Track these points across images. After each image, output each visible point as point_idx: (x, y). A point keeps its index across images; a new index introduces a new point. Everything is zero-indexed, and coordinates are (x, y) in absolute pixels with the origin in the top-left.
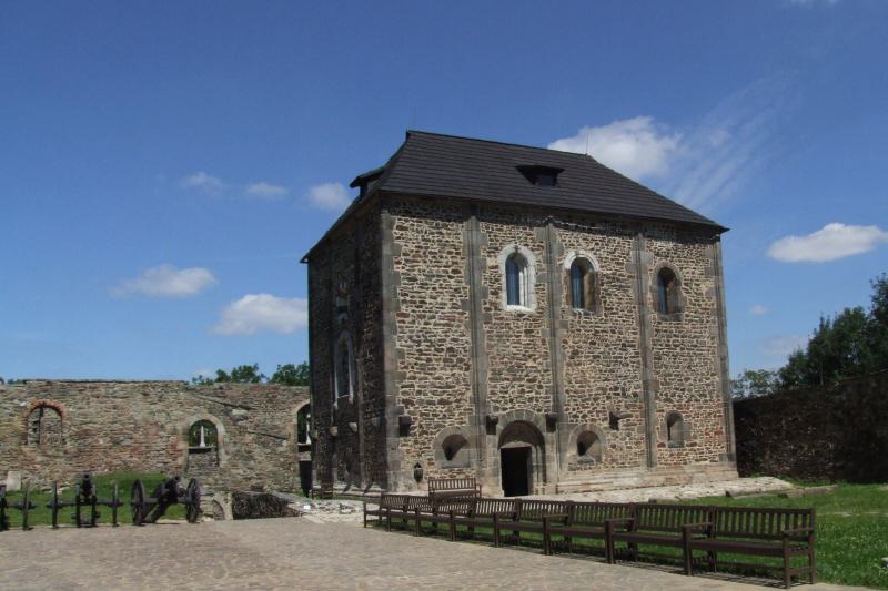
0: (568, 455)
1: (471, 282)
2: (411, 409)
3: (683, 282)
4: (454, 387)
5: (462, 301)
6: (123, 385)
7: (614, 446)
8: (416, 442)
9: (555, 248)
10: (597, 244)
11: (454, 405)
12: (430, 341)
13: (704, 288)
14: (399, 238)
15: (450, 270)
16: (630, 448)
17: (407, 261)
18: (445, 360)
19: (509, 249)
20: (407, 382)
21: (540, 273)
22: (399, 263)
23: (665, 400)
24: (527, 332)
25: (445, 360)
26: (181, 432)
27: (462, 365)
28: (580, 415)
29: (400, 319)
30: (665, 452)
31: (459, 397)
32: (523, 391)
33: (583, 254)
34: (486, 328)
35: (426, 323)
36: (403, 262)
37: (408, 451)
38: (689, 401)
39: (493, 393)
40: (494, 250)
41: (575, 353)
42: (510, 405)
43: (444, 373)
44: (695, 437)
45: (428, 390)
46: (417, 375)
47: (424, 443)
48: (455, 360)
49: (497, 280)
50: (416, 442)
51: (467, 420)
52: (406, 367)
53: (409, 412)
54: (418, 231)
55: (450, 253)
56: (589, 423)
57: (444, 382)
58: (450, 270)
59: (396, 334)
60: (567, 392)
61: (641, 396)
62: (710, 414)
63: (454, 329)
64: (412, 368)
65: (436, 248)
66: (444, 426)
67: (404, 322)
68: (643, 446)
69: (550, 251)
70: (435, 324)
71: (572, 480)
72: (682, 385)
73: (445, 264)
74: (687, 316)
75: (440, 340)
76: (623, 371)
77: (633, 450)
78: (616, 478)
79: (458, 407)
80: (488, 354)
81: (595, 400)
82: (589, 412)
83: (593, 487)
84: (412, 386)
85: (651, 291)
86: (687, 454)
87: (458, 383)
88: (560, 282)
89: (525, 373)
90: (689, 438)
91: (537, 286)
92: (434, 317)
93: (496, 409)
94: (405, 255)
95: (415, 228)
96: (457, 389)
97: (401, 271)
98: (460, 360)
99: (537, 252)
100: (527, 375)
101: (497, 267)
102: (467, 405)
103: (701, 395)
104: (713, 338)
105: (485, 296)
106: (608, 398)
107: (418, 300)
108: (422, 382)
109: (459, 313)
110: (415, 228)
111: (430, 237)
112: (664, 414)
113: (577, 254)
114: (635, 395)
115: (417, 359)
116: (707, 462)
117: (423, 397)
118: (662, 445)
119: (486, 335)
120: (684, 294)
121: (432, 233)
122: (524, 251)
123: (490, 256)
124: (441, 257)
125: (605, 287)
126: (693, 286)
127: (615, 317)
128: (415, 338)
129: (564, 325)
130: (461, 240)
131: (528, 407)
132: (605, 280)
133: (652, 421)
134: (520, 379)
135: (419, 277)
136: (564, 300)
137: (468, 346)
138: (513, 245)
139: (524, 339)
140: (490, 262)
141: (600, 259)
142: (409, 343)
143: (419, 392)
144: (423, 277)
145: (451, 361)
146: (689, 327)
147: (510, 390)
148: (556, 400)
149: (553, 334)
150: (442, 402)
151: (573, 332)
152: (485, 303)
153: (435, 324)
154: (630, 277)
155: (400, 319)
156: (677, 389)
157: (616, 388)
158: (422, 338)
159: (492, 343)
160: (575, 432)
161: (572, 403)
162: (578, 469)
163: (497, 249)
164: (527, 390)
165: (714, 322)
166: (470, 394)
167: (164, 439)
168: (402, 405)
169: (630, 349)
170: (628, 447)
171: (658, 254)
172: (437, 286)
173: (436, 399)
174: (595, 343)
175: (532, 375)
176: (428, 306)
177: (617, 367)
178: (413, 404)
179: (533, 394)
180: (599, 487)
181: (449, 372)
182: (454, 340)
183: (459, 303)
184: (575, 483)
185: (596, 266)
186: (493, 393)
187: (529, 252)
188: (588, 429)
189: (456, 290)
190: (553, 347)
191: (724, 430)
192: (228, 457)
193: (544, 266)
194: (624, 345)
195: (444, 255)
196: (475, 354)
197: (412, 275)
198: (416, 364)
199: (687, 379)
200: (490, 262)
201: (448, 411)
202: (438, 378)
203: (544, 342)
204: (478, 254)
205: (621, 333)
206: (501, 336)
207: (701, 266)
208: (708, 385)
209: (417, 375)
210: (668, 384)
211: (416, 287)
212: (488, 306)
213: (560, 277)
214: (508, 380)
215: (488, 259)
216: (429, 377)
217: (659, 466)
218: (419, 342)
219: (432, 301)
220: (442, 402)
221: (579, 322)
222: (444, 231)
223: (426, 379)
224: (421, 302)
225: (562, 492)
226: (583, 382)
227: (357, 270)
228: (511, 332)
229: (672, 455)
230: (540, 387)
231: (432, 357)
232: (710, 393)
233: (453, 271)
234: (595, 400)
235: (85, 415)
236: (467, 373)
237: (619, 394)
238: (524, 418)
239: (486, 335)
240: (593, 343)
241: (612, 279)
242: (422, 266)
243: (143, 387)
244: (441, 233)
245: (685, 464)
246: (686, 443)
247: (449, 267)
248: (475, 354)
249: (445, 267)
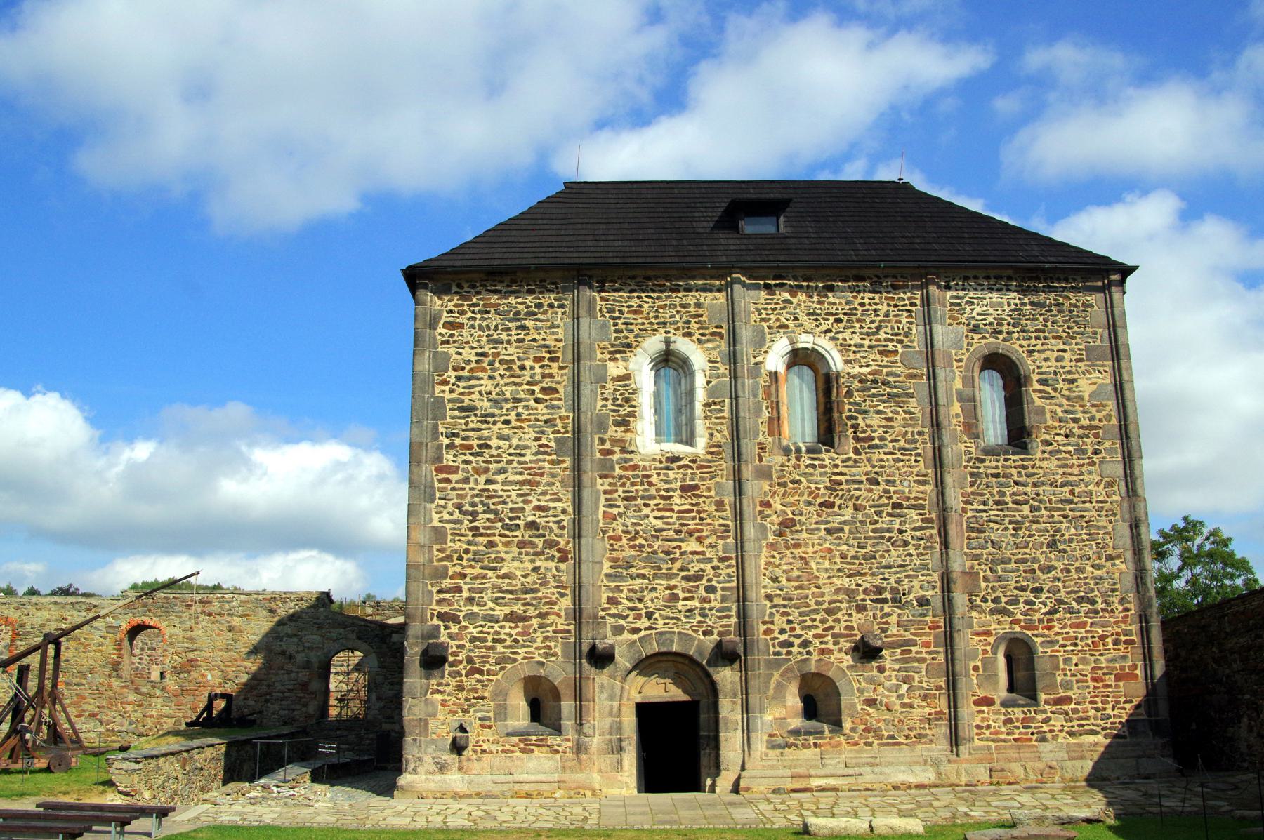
0: (768, 718)
1: (576, 407)
2: (454, 629)
3: (1035, 377)
4: (537, 591)
5: (557, 441)
6: (243, 597)
7: (871, 703)
8: (460, 688)
9: (745, 334)
10: (839, 321)
11: (535, 622)
12: (496, 512)
13: (1085, 387)
14: (443, 343)
15: (537, 389)
16: (911, 706)
17: (459, 378)
18: (521, 545)
19: (654, 344)
20: (447, 583)
21: (714, 382)
22: (445, 383)
23: (992, 612)
24: (684, 489)
25: (521, 545)
26: (316, 665)
27: (553, 552)
28: (797, 641)
29: (441, 476)
30: (995, 717)
31: (544, 609)
32: (675, 597)
33: (806, 341)
34: (602, 485)
35: (488, 482)
36: (453, 380)
37: (444, 703)
38: (1053, 611)
39: (612, 601)
40: (624, 349)
41: (788, 524)
42: (644, 623)
43: (517, 566)
44: (1067, 685)
45: (487, 596)
46: (468, 571)
47: (476, 690)
48: (540, 543)
49: (627, 400)
50: (460, 688)
51: (559, 650)
52: (449, 558)
53: (450, 636)
54: (481, 328)
55: (538, 359)
56: (815, 657)
57: (517, 584)
58: (537, 389)
59: (432, 502)
60: (769, 597)
61: (937, 602)
62: (1103, 638)
63: (540, 489)
64: (460, 558)
65: (512, 352)
66: (515, 660)
67: (448, 481)
68: (942, 704)
69: (733, 340)
70: (505, 483)
71: (772, 767)
72: (1035, 580)
73: (528, 378)
74: (1048, 443)
75: (512, 510)
76: (895, 556)
77: (916, 712)
78: (872, 765)
79: (541, 626)
80: (604, 532)
82: (816, 636)
83: (815, 782)
84: (459, 590)
85: (961, 398)
86: (1046, 721)
87: (544, 583)
88: (755, 396)
89: (678, 565)
90: (1052, 686)
91: (707, 405)
92: (503, 471)
93: (618, 630)
94: (455, 369)
95: (476, 323)
96: (540, 594)
97: (447, 396)
98: (551, 544)
99: (710, 345)
100: (682, 569)
101: (627, 377)
102: (561, 624)
103: (1080, 600)
104: (1110, 485)
106: (861, 608)
107: (475, 442)
108: (477, 584)
109: (552, 462)
110: (476, 323)
111: (504, 336)
112: (991, 640)
113: (792, 343)
114: (923, 602)
115: (469, 543)
117: (476, 609)
119: (603, 497)
120: (1038, 402)
121: (509, 329)
122: (684, 346)
123: (615, 360)
124: (522, 368)
125: (857, 397)
127: (876, 455)
128: (468, 508)
129: (764, 474)
130: (561, 336)
131: (684, 626)
132: (856, 385)
133: (958, 654)
134: (669, 576)
135: (478, 404)
136: (763, 428)
137: (567, 520)
138: (660, 336)
139: (678, 502)
140: (614, 369)
141: (845, 348)
142: (457, 515)
143: (470, 600)
144: (487, 404)
145: (533, 545)
146: (1052, 464)
147: (648, 596)
148: (743, 614)
149: (739, 490)
150: (513, 618)
151: (784, 485)
152: (602, 441)
154: (911, 376)
155: (441, 476)
156: (1023, 589)
157: (879, 590)
158: (480, 508)
159: (615, 511)
160: (782, 675)
161: (780, 621)
162: (789, 746)
163: (629, 346)
164: (682, 595)
165: (1110, 451)
166: (566, 602)
167: (293, 675)
168: (436, 622)
169: (913, 514)
170: (903, 705)
171: (975, 329)
172: (512, 416)
173: (500, 612)
174: (832, 505)
175: (694, 568)
176: (494, 452)
177: (881, 548)
178: (456, 620)
179: (696, 603)
180: (831, 782)
182: (539, 508)
183: (552, 444)
184: (781, 772)
185: (836, 362)
186: (612, 601)
187: (694, 346)
188: (813, 668)
189: (546, 422)
190: (739, 514)
191: (1138, 672)
192: (382, 704)
193: (723, 369)
194: (897, 506)
195: (528, 364)
196: (577, 535)
197: (467, 403)
198: (467, 551)
199: (1050, 569)
200: (614, 369)
201: (524, 633)
202: (505, 576)
203: (720, 505)
204: (591, 358)
205: (890, 483)
206: (634, 499)
207: (1077, 345)
208: (1098, 580)
209: (468, 571)
210: (1000, 578)
211: (473, 422)
212: (607, 446)
213: (756, 385)
214: (643, 576)
215: (610, 365)
216: (490, 573)
217: (977, 743)
218: (474, 515)
219: (501, 443)
220: (513, 618)
221: (796, 467)
223: (484, 577)
224: (480, 446)
225: (747, 789)
226: (805, 577)
228: (653, 491)
229: (1008, 721)
230: (711, 589)
231: (497, 539)
232: (1104, 595)
233: (543, 390)
234: (829, 612)
235: (190, 639)
236: (563, 566)
237: (885, 601)
238: (675, 648)
239: (603, 497)
240: (827, 505)
241: (868, 383)
242: (487, 385)
243: (270, 600)
244: (523, 328)
245: (1043, 740)
246: (1042, 696)
247: (536, 383)
248: (577, 535)
249: (529, 383)
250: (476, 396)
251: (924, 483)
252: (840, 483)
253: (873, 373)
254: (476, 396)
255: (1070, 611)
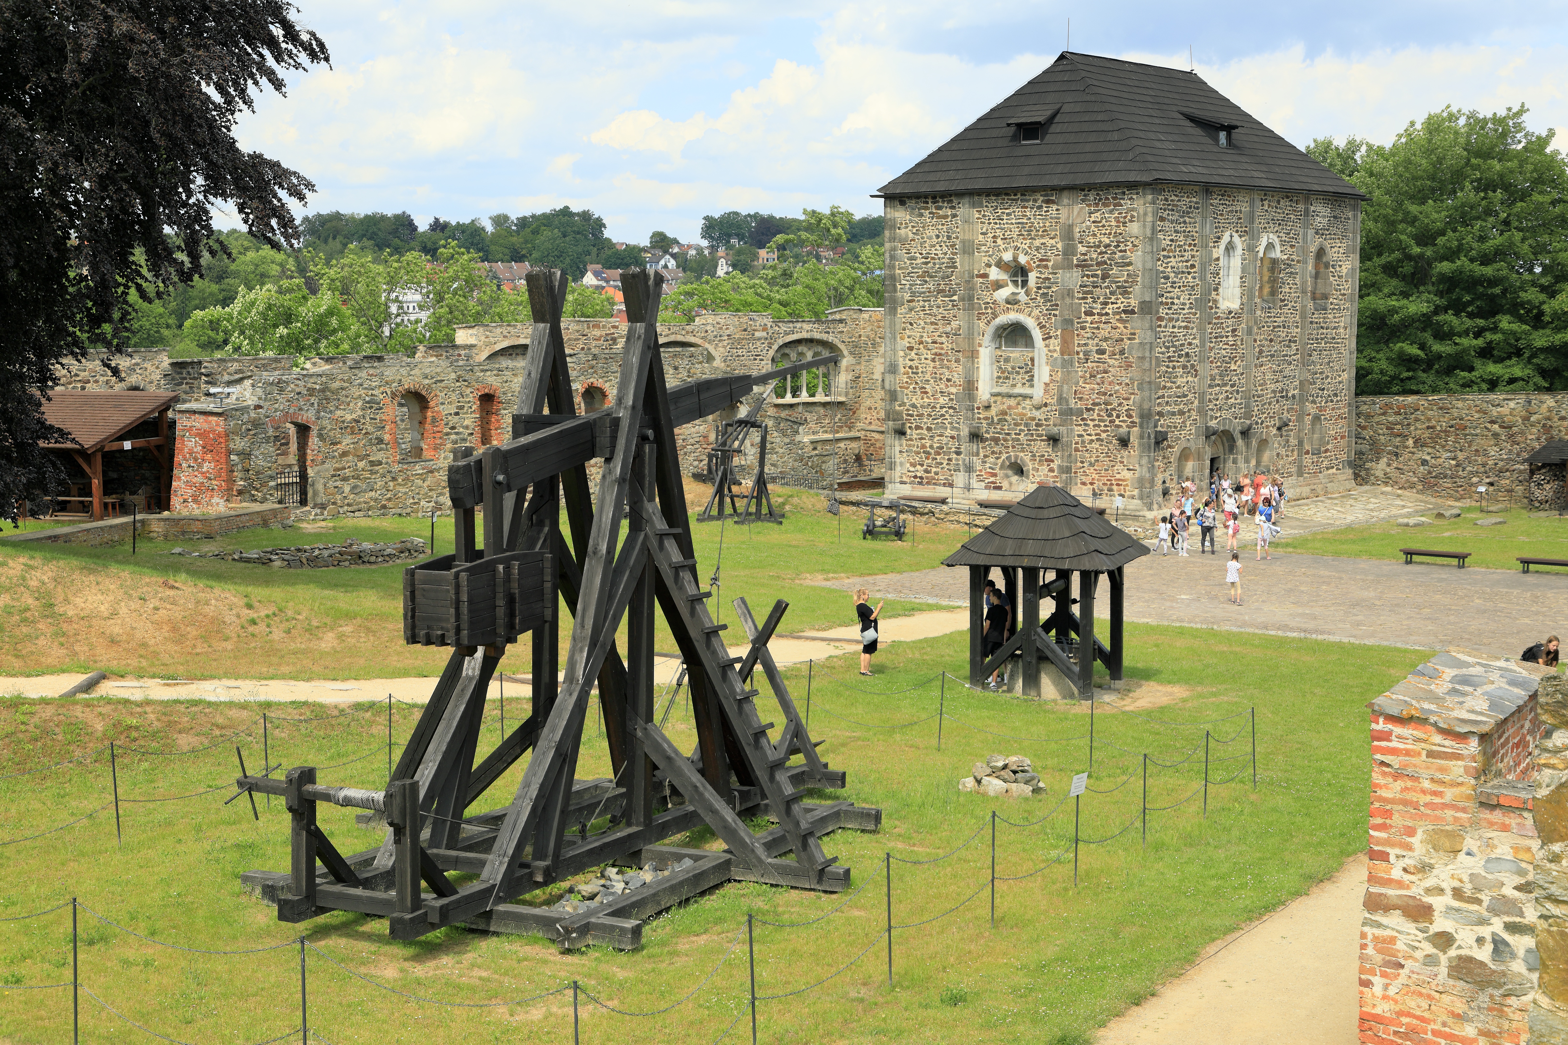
20: (1160, 393)
22: (1159, 260)
35: (1174, 327)
39: (1210, 401)
41: (1261, 352)
44: (1328, 443)
52: (1160, 377)
67: (1160, 326)
70: (1180, 327)
81: (1270, 404)
93: (1212, 417)
97: (1161, 269)
98: (1193, 366)
101: (1218, 259)
105: (1210, 294)
116: (1334, 470)
118: (1307, 453)
126: (1338, 269)
134: (1225, 385)
150: (1181, 413)
153: (1180, 327)
154: (1298, 262)
163: (1219, 238)
166: (1196, 402)
171: (1317, 233)
179: (1233, 400)
181: (1185, 380)
199: (1327, 377)
203: (1242, 340)
208: (1340, 382)
218: (1168, 348)
220: (1181, 413)
222: (1187, 220)
227: (1069, 251)
244: (1185, 222)
250: (1169, 269)
251: (1297, 327)
252: (1274, 327)
253: (1288, 259)
254: (1169, 269)
255: (1332, 401)
